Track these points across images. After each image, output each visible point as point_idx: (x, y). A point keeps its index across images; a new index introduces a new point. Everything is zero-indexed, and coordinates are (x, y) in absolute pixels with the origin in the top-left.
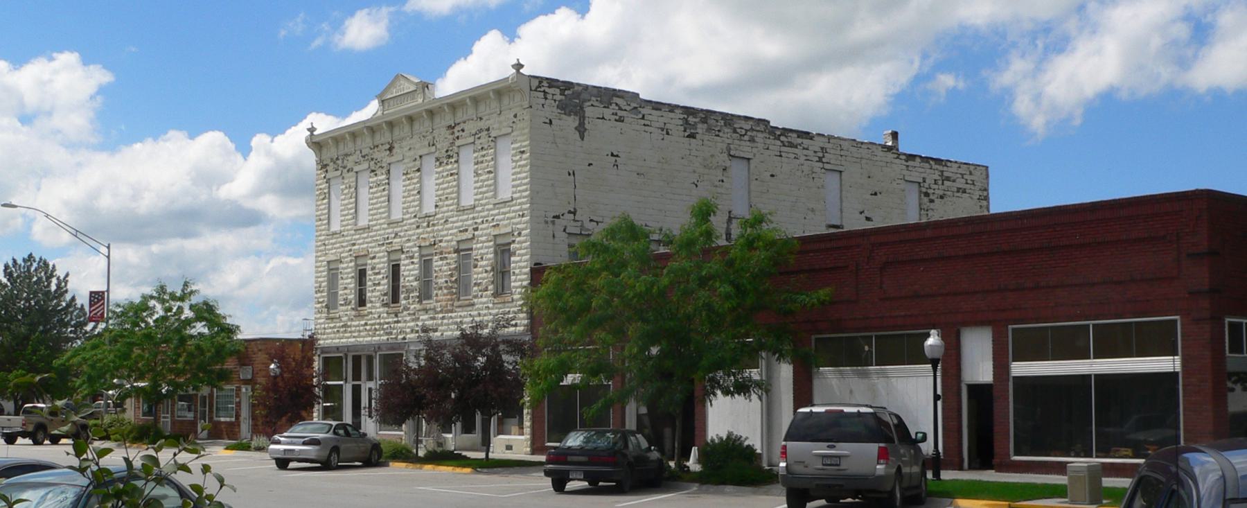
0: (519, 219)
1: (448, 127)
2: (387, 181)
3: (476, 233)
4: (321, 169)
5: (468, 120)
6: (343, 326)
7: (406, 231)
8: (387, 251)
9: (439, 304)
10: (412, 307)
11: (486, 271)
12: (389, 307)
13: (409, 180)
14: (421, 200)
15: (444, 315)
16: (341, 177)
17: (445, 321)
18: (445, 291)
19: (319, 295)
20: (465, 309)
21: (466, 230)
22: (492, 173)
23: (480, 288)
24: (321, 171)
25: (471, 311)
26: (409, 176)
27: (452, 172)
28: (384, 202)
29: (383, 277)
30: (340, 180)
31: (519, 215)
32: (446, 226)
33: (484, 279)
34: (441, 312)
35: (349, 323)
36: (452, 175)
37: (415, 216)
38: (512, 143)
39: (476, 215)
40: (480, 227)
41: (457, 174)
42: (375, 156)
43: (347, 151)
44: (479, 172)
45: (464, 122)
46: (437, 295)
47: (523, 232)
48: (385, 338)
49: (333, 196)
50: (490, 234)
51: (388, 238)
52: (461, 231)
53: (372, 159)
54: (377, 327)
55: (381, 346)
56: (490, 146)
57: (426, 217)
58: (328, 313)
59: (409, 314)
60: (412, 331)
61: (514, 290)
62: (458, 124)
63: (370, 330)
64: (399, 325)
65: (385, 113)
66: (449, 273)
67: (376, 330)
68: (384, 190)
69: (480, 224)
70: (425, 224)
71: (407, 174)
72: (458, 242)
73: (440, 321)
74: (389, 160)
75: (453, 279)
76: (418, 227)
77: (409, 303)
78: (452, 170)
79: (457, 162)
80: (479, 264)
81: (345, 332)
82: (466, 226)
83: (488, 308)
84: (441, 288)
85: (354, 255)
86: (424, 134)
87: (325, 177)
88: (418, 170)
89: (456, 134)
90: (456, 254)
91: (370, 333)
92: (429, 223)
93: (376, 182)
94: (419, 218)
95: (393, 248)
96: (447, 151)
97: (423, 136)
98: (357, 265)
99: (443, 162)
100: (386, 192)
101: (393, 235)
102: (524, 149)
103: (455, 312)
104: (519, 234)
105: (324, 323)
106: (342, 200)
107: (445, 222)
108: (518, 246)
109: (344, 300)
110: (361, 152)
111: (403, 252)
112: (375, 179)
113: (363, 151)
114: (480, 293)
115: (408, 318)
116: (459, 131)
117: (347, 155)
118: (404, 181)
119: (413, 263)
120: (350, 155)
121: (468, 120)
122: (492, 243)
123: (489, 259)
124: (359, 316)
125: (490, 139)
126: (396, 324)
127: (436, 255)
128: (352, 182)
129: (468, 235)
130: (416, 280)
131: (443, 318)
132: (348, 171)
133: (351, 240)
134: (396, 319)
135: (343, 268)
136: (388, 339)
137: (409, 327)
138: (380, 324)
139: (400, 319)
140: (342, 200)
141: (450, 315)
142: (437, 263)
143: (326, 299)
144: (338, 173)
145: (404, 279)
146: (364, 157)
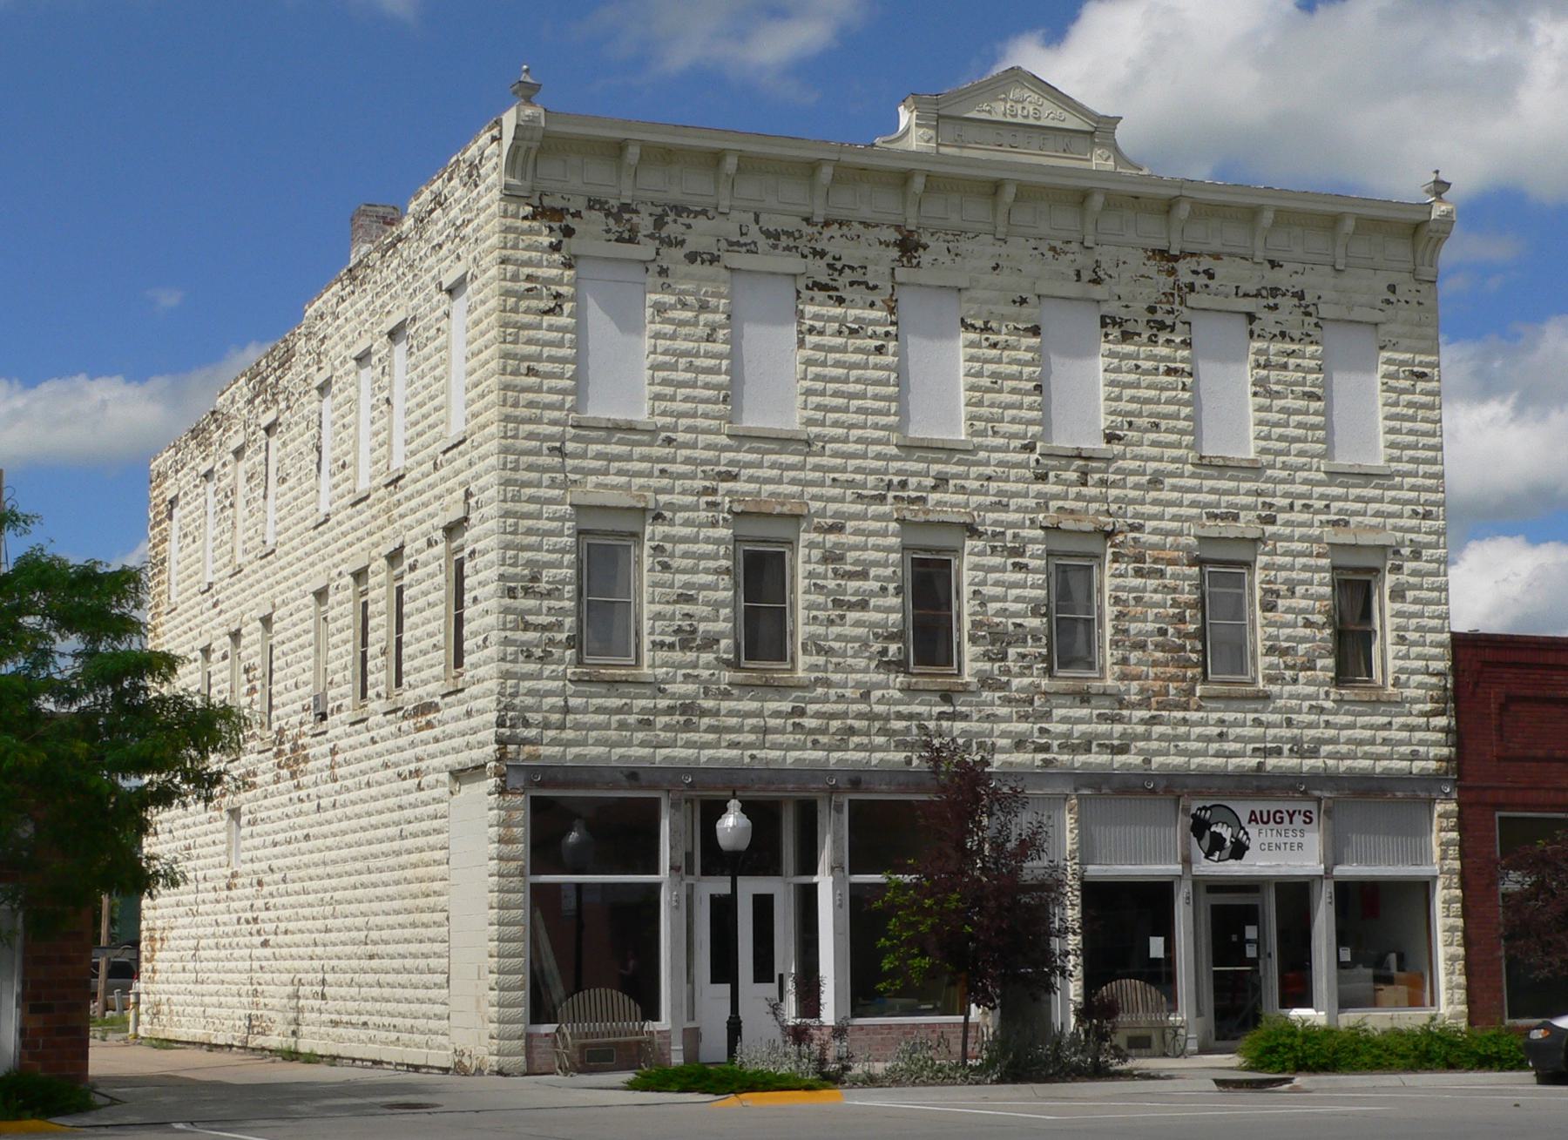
0: (1414, 522)
1: (1153, 251)
2: (892, 329)
3: (1269, 529)
4: (534, 217)
5: (1231, 255)
6: (670, 711)
7: (989, 478)
8: (902, 521)
9: (1135, 685)
10: (1016, 682)
11: (1308, 624)
12: (907, 673)
13: (994, 346)
14: (1044, 408)
15: (1154, 713)
16: (653, 268)
17: (1158, 730)
18: (1159, 655)
19: (531, 603)
20: (1235, 704)
21: (1236, 518)
22: (1319, 399)
23: (1289, 660)
24: (535, 224)
25: (1256, 711)
26: (994, 338)
27: (1173, 365)
28: (886, 383)
29: (884, 589)
30: (653, 279)
31: (1416, 513)
32: (1153, 494)
33: (1304, 640)
34: (1144, 704)
35: (709, 704)
36: (1169, 372)
37: (1029, 448)
38: (1382, 348)
39: (1264, 486)
40: (1281, 517)
41: (1190, 375)
42: (832, 249)
43: (675, 195)
44: (1276, 388)
45: (1217, 256)
46: (1124, 661)
47: (1426, 553)
48: (900, 756)
49: (596, 315)
50: (1318, 540)
51: (903, 485)
52: (1216, 516)
53: (822, 254)
54: (857, 724)
55: (864, 777)
56: (1308, 335)
57: (1079, 457)
58: (579, 662)
59: (1008, 701)
60: (1019, 744)
61: (1403, 677)
62: (1193, 255)
63: (824, 731)
64: (959, 726)
65: (943, 150)
66: (1171, 611)
67: (852, 731)
68: (879, 350)
69: (1282, 510)
70: (1074, 476)
71: (986, 329)
72: (1201, 539)
73: (1141, 729)
74: (902, 274)
75: (1192, 628)
76: (1042, 478)
77: (1008, 672)
78: (1174, 360)
79: (1187, 344)
80: (1280, 602)
81: (688, 726)
82: (1235, 506)
83: (1322, 710)
84: (1142, 646)
85: (737, 508)
86: (1058, 244)
87: (555, 248)
88: (1035, 331)
89: (1185, 277)
90: (1196, 569)
91: (823, 739)
92: (1086, 474)
93: (842, 321)
94: (1041, 455)
95: (932, 517)
96: (1152, 310)
97: (1053, 249)
98: (736, 539)
99: (1139, 335)
100: (889, 359)
101: (930, 482)
102: (1426, 370)
103: (1199, 709)
104: (1416, 555)
105: (562, 693)
106: (657, 336)
107: (1150, 482)
108: (1412, 580)
109: (679, 630)
110: (757, 221)
111: (972, 530)
112: (839, 311)
113: (763, 217)
114: (1289, 674)
115: (1003, 711)
116: (1195, 272)
117: (679, 210)
118: (971, 344)
119: (1019, 567)
120: (704, 212)
121: (1231, 255)
122: (1325, 562)
123: (1320, 598)
124: (767, 685)
125: (1308, 319)
126: (945, 724)
127: (1115, 561)
128: (719, 296)
129: (1246, 525)
130: (1035, 613)
131: (1153, 721)
132: (692, 257)
133: (717, 463)
134: (948, 709)
135: (666, 538)
136: (909, 761)
137: (1004, 734)
138: (871, 717)
139: (958, 708)
140: (657, 336)
141: (1180, 714)
142: (1110, 579)
143: (569, 621)
144: (646, 250)
145: (983, 604)
146: (775, 236)
